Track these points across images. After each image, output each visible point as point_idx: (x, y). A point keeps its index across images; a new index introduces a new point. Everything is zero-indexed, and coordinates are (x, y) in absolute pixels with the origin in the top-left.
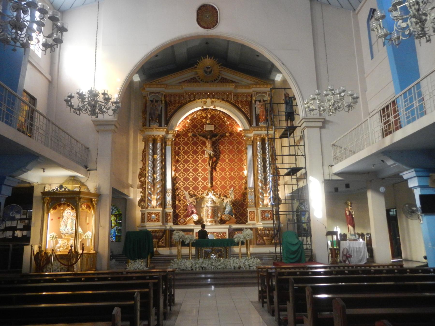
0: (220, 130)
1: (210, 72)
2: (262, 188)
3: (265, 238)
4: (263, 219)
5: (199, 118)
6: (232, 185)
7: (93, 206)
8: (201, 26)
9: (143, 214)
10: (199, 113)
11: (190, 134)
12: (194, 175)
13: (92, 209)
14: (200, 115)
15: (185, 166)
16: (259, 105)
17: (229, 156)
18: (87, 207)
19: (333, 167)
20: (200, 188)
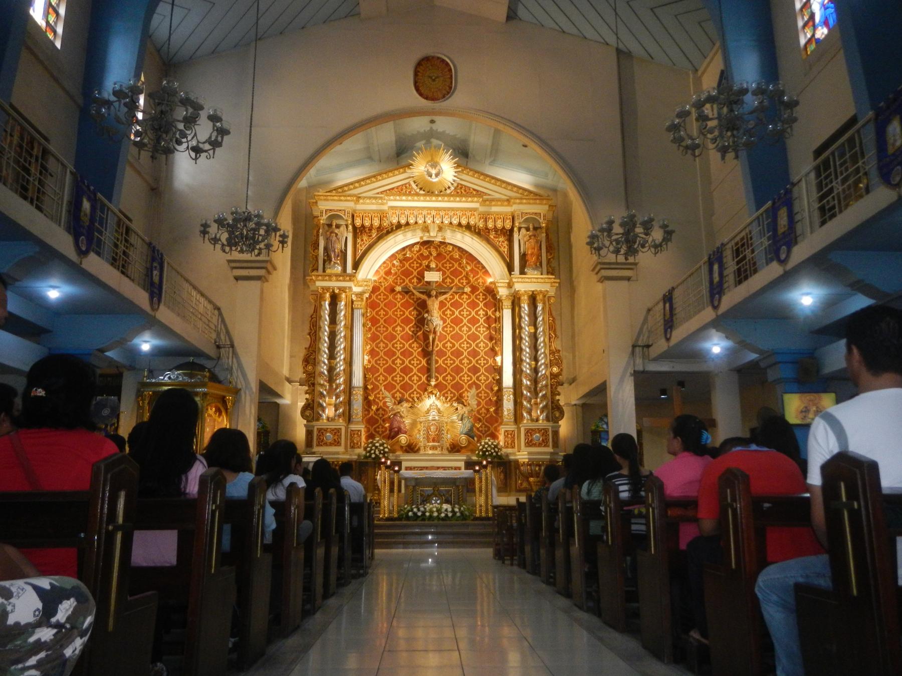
0: (453, 281)
1: (437, 175)
2: (528, 389)
3: (531, 479)
4: (529, 444)
5: (415, 257)
6: (474, 383)
7: (226, 409)
8: (421, 95)
9: (309, 433)
10: (416, 248)
11: (398, 289)
12: (403, 362)
13: (224, 414)
14: (418, 252)
15: (387, 345)
16: (525, 236)
17: (470, 329)
18: (216, 411)
19: (651, 349)
20: (415, 387)
